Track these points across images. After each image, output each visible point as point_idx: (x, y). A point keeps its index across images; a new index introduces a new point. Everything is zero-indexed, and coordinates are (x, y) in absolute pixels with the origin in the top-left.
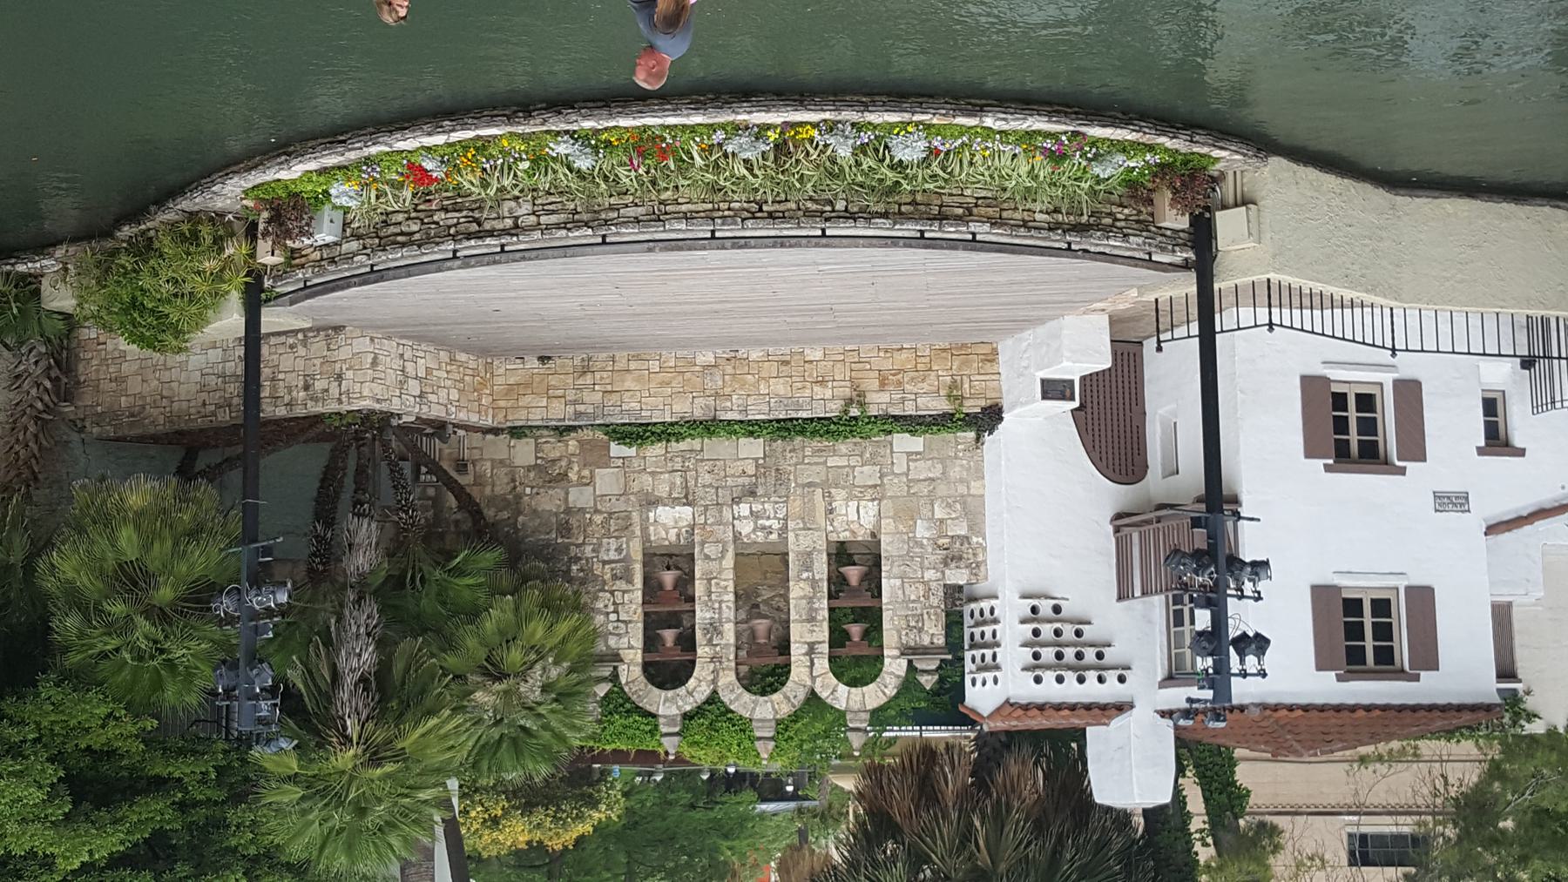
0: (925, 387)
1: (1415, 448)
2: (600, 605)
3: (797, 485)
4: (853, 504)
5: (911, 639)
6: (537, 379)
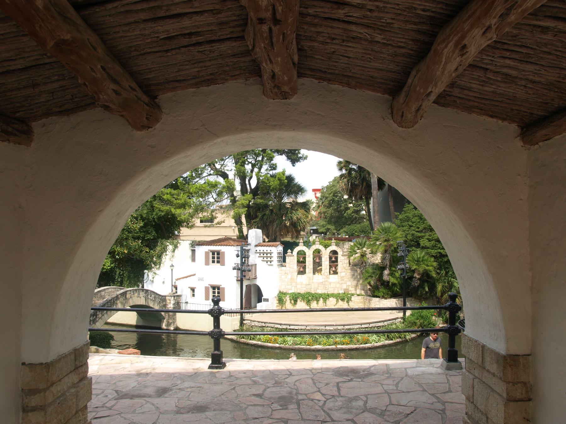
1: (207, 289)
5: (292, 257)
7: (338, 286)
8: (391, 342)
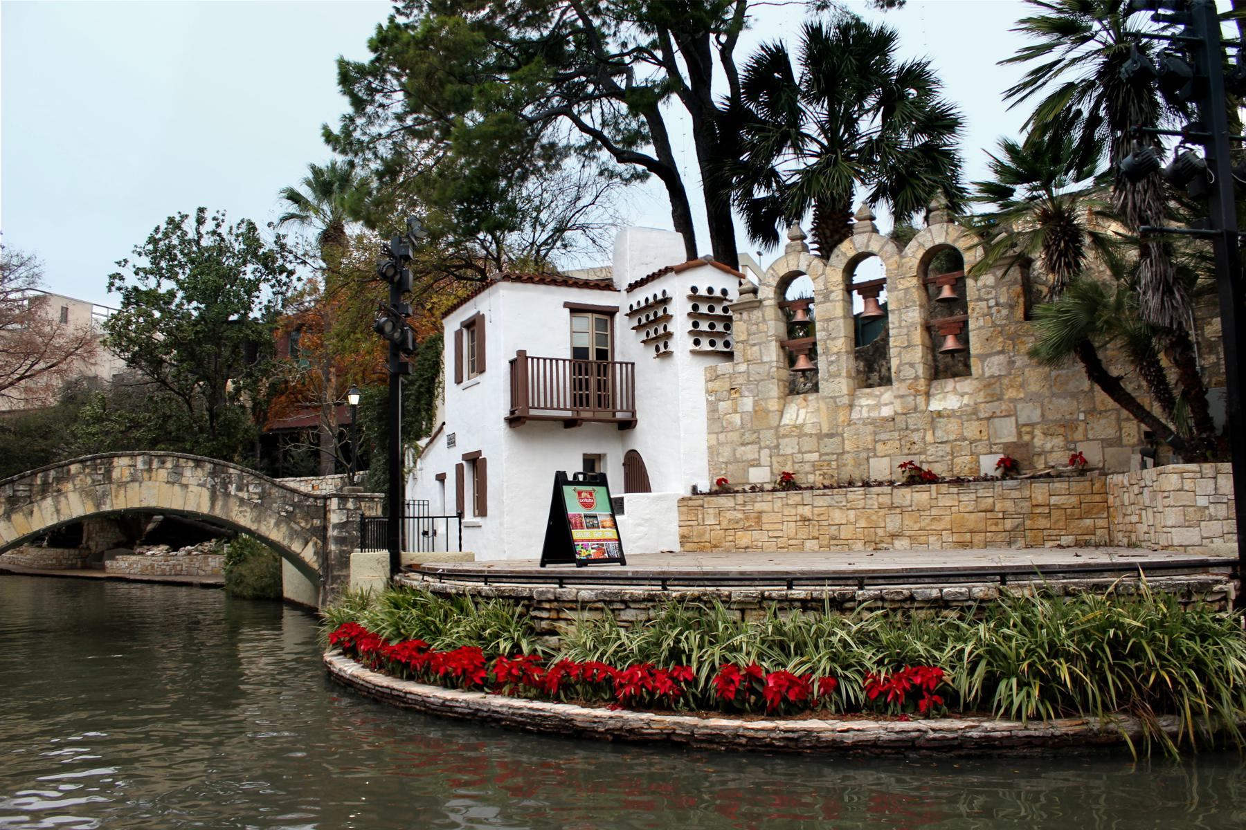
0: (729, 515)
3: (842, 435)
4: (800, 421)
5: (756, 314)
6: (1061, 524)
7: (972, 429)
8: (1063, 726)
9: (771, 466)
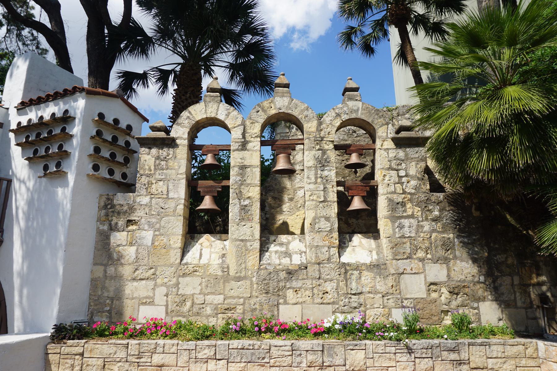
2: (413, 183)
4: (204, 261)
9: (167, 306)
